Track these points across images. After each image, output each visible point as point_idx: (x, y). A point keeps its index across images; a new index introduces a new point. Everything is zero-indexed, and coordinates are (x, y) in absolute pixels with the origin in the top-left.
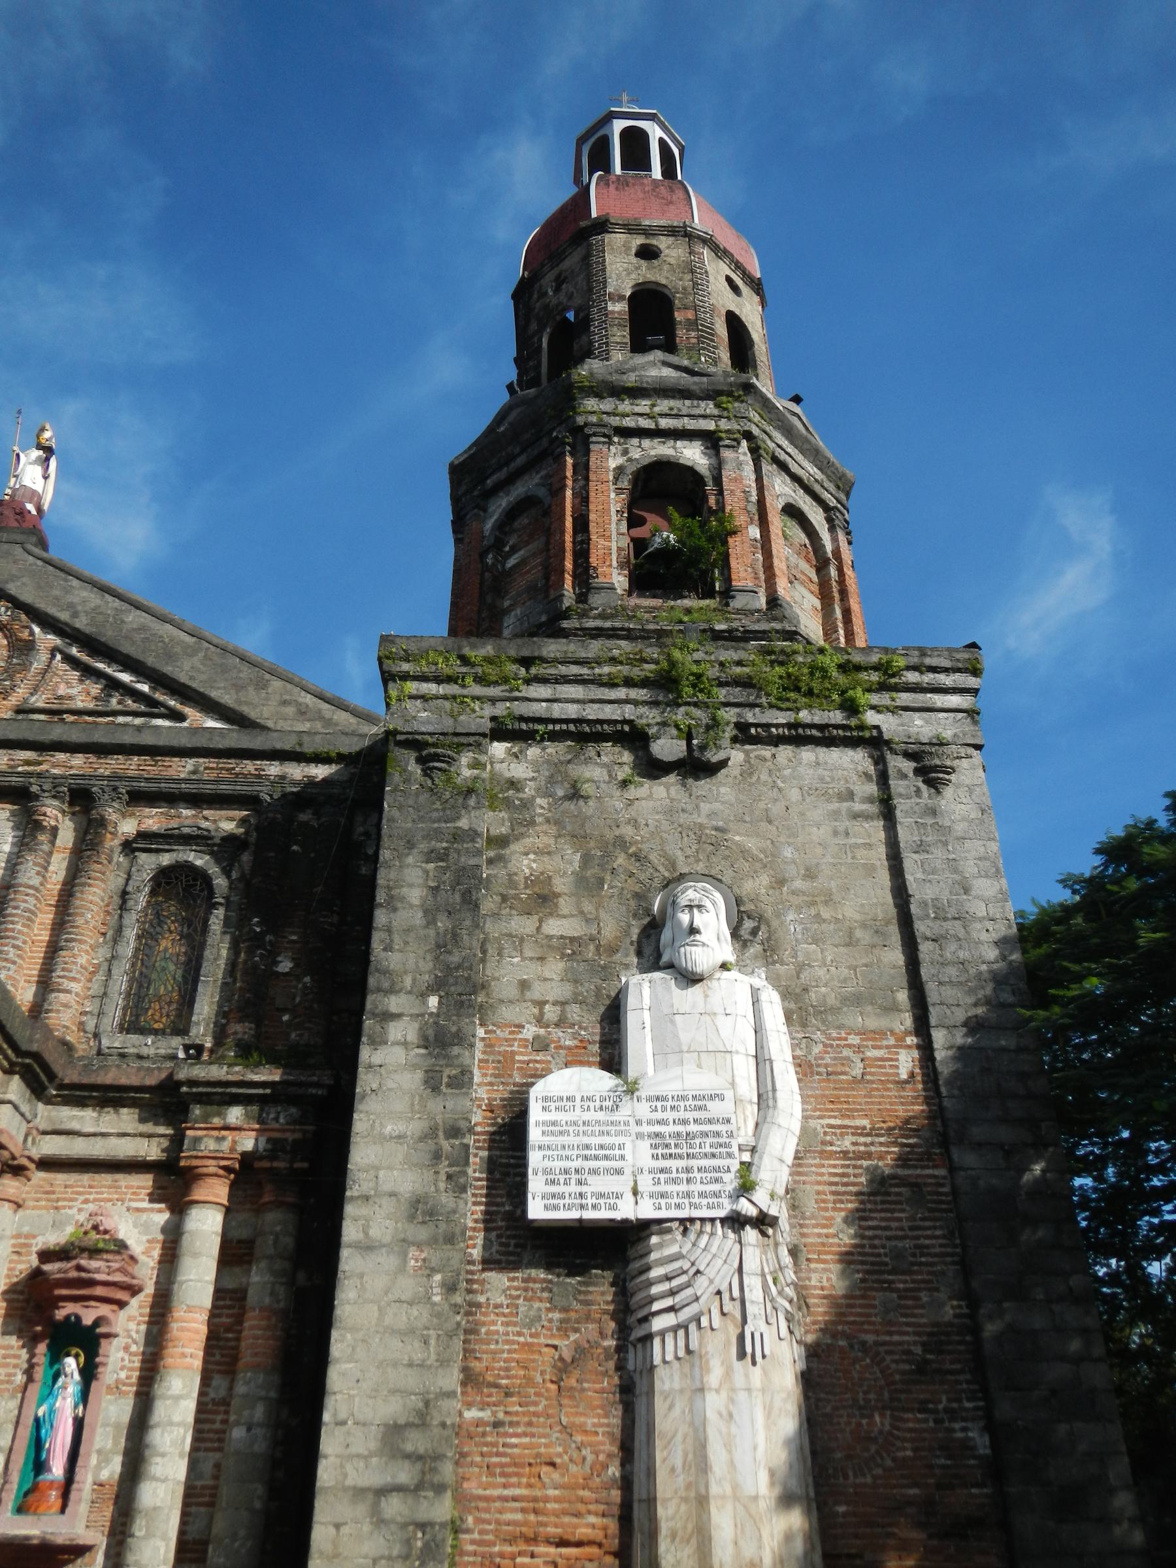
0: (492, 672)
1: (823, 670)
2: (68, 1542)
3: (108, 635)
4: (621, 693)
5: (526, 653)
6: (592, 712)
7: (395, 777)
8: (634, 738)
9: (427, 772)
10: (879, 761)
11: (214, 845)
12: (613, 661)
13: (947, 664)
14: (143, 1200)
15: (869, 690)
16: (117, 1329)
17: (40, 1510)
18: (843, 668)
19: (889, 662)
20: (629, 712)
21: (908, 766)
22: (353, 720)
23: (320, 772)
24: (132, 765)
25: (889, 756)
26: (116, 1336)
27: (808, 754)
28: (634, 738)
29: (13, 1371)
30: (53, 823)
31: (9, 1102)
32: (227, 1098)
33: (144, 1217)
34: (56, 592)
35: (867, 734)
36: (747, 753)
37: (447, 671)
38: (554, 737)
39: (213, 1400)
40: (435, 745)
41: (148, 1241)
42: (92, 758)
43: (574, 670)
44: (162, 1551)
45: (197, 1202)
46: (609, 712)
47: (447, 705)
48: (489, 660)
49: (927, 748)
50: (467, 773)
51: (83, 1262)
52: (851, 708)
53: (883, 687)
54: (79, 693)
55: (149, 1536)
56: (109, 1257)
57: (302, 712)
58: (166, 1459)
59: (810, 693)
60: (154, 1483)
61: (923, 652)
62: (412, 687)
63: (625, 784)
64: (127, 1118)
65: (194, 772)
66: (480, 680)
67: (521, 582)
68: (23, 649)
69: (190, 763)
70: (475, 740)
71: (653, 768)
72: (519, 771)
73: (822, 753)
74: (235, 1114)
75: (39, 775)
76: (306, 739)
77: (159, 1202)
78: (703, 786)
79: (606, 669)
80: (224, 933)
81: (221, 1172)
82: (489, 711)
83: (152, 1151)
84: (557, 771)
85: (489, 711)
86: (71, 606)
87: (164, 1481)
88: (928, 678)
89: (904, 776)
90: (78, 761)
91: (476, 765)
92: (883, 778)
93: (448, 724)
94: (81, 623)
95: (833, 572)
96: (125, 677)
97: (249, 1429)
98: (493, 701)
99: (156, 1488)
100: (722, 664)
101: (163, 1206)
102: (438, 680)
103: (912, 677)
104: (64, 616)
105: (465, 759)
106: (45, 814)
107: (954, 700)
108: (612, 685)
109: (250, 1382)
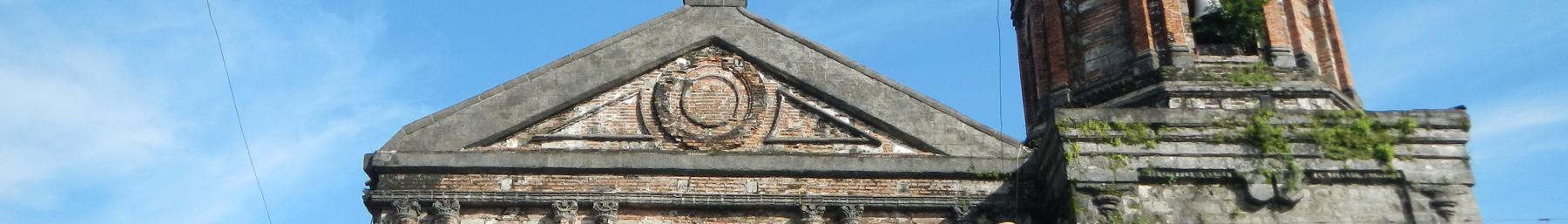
0: (1133, 134)
1: (1362, 131)
3: (815, 81)
4: (1222, 148)
5: (1155, 120)
6: (1206, 164)
7: (1081, 215)
8: (1236, 182)
9: (1103, 212)
10: (1404, 196)
12: (1216, 125)
13: (1445, 122)
15: (1392, 144)
18: (1375, 127)
19: (1406, 123)
20: (1230, 163)
21: (1425, 200)
22: (999, 143)
23: (990, 188)
24: (860, 187)
25: (1411, 193)
27: (1354, 191)
28: (1236, 182)
34: (771, 47)
35: (1393, 176)
36: (1312, 191)
37: (1102, 135)
38: (1180, 181)
40: (1105, 192)
42: (833, 182)
43: (1189, 132)
46: (1217, 164)
47: (1106, 160)
48: (1130, 126)
49: (1436, 188)
50: (1129, 211)
52: (1382, 158)
53: (1403, 141)
54: (804, 127)
57: (962, 138)
59: (1353, 147)
61: (1428, 113)
62: (1080, 146)
63: (1233, 215)
65: (903, 190)
66: (1126, 140)
67: (1095, 26)
68: (756, 93)
69: (899, 183)
70: (1129, 187)
71: (1251, 204)
72: (1160, 207)
73: (1362, 188)
75: (803, 196)
76: (975, 163)
78: (1285, 217)
79: (1211, 131)
82: (1136, 164)
84: (1185, 208)
85: (1136, 164)
86: (784, 58)
88: (1433, 134)
89: (1423, 209)
90: (823, 183)
91: (1133, 205)
92: (1408, 208)
93: (1108, 175)
94: (795, 72)
95: (1321, 9)
96: (831, 112)
98: (1137, 156)
100: (1291, 127)
102: (1097, 141)
103: (1422, 133)
104: (782, 66)
105: (1125, 200)
107: (1451, 150)
108: (1216, 143)
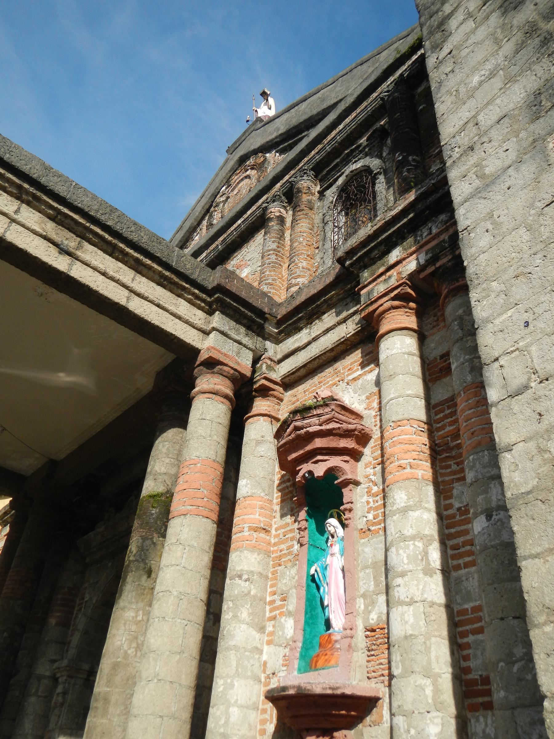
2: (329, 692)
11: (365, 148)
14: (358, 370)
16: (360, 478)
17: (320, 664)
26: (357, 483)
29: (291, 543)
30: (278, 214)
31: (214, 329)
32: (383, 248)
33: (360, 381)
39: (459, 509)
41: (368, 398)
44: (429, 691)
45: (383, 336)
51: (298, 424)
55: (409, 672)
56: (319, 411)
58: (406, 578)
60: (400, 608)
64: (329, 319)
74: (395, 255)
77: (368, 365)
80: (389, 188)
81: (396, 303)
83: (349, 329)
87: (412, 602)
97: (489, 517)
99: (403, 614)
101: (373, 365)
106: (271, 212)
109: (474, 466)
